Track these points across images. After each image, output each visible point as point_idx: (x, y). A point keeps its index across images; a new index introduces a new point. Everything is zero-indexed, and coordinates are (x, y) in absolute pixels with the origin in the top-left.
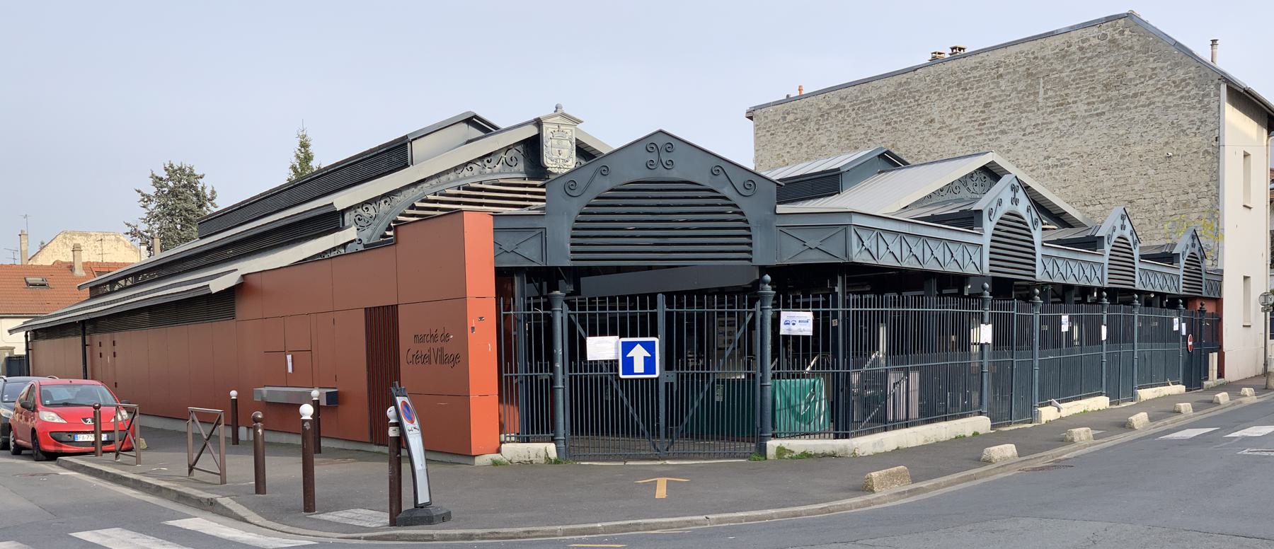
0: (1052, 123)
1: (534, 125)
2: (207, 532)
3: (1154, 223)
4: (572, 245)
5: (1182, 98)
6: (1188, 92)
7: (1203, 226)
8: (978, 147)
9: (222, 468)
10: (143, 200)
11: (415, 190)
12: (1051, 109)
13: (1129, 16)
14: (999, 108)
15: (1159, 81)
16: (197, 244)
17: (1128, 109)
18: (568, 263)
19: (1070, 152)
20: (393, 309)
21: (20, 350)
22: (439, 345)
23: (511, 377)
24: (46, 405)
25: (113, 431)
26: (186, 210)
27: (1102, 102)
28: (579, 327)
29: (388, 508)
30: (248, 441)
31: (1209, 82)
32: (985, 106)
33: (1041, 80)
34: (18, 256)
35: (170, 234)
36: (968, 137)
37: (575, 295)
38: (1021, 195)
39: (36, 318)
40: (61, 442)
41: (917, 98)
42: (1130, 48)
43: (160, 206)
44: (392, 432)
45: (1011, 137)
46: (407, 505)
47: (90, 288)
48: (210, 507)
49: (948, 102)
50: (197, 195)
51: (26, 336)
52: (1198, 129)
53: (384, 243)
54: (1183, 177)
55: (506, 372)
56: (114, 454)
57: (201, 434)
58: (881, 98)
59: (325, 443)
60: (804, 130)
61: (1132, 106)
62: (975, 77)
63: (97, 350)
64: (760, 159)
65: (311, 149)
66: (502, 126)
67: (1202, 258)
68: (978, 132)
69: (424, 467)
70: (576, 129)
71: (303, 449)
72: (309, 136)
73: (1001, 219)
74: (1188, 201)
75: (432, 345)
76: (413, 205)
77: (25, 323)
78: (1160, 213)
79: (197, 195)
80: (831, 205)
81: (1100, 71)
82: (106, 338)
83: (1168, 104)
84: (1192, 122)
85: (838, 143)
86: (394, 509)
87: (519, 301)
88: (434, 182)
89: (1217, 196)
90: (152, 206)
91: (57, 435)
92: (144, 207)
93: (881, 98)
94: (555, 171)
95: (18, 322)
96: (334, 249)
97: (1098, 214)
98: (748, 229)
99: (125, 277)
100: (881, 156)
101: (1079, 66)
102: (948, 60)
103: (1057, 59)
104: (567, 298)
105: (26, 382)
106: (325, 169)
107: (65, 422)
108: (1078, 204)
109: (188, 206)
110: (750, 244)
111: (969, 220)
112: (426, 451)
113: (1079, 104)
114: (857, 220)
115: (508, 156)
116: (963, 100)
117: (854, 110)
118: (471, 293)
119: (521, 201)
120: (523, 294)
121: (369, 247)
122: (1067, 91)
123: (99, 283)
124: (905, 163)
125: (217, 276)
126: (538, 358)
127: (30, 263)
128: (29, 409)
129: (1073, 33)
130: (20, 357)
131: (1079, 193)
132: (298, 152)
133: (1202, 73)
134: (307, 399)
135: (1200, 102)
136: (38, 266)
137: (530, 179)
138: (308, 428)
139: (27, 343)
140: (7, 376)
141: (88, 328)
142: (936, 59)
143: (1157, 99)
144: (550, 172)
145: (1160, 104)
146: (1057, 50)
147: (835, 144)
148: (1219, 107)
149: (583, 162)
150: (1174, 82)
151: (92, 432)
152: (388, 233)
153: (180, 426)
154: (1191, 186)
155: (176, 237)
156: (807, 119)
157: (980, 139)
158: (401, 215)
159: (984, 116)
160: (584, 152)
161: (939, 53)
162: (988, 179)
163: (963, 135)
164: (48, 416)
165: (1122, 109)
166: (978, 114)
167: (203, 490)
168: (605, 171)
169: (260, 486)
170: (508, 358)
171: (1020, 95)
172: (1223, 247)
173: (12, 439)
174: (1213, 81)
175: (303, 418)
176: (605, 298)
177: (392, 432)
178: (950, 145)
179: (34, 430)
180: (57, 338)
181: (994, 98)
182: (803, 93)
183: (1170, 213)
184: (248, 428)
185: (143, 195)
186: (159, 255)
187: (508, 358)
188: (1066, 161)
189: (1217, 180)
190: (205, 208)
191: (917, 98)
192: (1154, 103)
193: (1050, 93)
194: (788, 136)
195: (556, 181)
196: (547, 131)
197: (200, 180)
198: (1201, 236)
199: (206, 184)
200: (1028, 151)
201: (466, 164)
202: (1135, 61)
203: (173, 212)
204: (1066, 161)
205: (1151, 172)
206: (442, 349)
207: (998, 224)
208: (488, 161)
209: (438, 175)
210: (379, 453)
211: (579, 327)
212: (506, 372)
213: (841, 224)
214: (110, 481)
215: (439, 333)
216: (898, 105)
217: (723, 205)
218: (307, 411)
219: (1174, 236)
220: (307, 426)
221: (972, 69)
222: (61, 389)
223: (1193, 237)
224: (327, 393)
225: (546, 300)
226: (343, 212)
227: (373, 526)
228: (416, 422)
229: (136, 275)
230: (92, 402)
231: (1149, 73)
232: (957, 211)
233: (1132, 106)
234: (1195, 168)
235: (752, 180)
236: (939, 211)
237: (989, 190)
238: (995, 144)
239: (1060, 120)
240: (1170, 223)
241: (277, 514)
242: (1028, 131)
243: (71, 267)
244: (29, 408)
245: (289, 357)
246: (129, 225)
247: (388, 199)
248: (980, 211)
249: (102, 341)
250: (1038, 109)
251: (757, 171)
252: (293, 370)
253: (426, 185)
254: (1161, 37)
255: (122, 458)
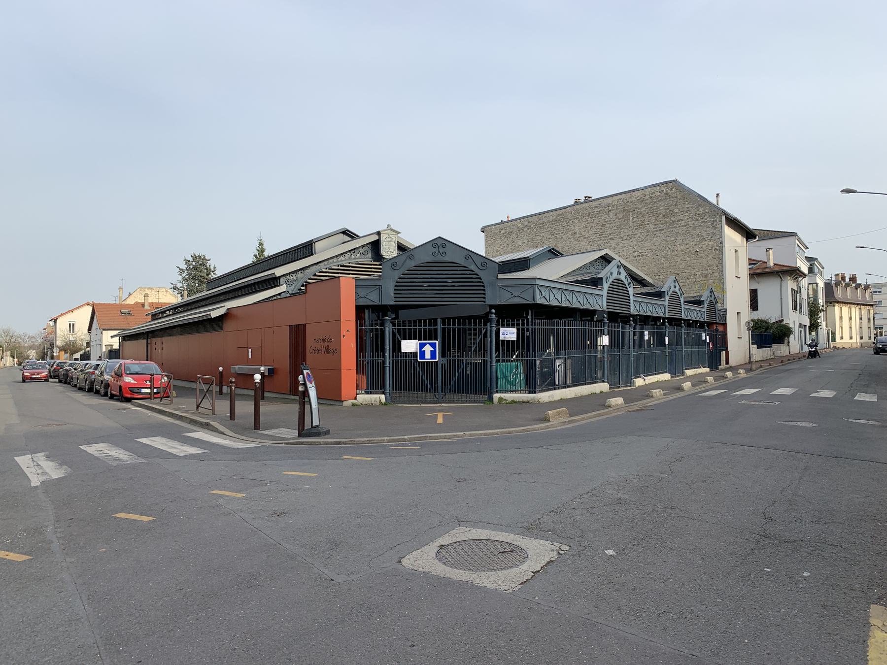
0: (636, 234)
1: (377, 234)
2: (204, 439)
3: (690, 285)
4: (394, 294)
5: (702, 222)
6: (706, 219)
7: (716, 286)
8: (599, 246)
9: (213, 407)
10: (180, 272)
11: (316, 267)
12: (636, 227)
13: (675, 181)
14: (609, 227)
15: (691, 214)
16: (205, 293)
17: (675, 227)
18: (392, 303)
19: (646, 249)
20: (304, 325)
21: (116, 346)
22: (326, 344)
23: (363, 360)
24: (127, 374)
25: (160, 388)
26: (201, 277)
27: (662, 224)
28: (397, 335)
29: (297, 428)
30: (227, 393)
31: (716, 215)
32: (602, 226)
33: (631, 213)
34: (117, 300)
35: (192, 288)
36: (593, 241)
37: (396, 319)
38: (622, 270)
39: (125, 330)
40: (134, 393)
41: (567, 222)
42: (676, 197)
43: (188, 275)
44: (301, 388)
45: (616, 241)
46: (307, 426)
47: (152, 315)
48: (206, 426)
49: (583, 224)
50: (207, 269)
51: (119, 339)
52: (711, 238)
53: (300, 293)
54: (705, 261)
55: (360, 358)
56: (160, 399)
57: (203, 390)
58: (549, 222)
59: (266, 395)
60: (510, 238)
61: (677, 226)
62: (597, 211)
63: (154, 346)
64: (488, 252)
65: (264, 246)
66: (361, 235)
67: (716, 303)
68: (599, 239)
69: (317, 406)
70: (398, 237)
71: (255, 397)
72: (263, 240)
73: (612, 282)
74: (708, 274)
75: (323, 344)
76: (315, 274)
77: (119, 332)
78: (694, 280)
79: (207, 269)
80: (525, 275)
81: (661, 208)
82: (158, 340)
83: (696, 225)
84: (708, 234)
85: (527, 244)
86: (300, 428)
87: (367, 322)
88: (326, 263)
89: (722, 271)
90: (184, 274)
91: (132, 389)
92: (180, 275)
93: (549, 222)
94: (387, 257)
95: (116, 332)
96: (274, 296)
97: (661, 280)
98: (484, 286)
99: (169, 310)
100: (550, 251)
101: (650, 206)
102: (583, 203)
103: (638, 202)
104: (392, 321)
105: (118, 362)
106: (271, 256)
107: (136, 382)
108: (651, 275)
109: (202, 274)
110: (484, 294)
111: (596, 282)
112: (318, 398)
113: (650, 225)
114: (539, 282)
115: (363, 250)
116: (591, 223)
117: (535, 228)
118: (343, 317)
119: (367, 272)
120: (369, 319)
121: (292, 295)
122: (644, 219)
123: (156, 313)
124: (562, 254)
125: (215, 309)
126: (377, 351)
127: (123, 303)
128: (118, 376)
129: (646, 190)
130: (116, 349)
131: (651, 270)
132: (258, 248)
133: (712, 210)
134: (258, 371)
135: (712, 224)
136: (127, 305)
137: (374, 261)
138: (258, 386)
139: (120, 342)
140: (109, 359)
141: (150, 335)
142: (577, 202)
143: (690, 223)
144: (384, 258)
145: (691, 225)
146: (639, 198)
147: (526, 245)
148: (721, 226)
149: (401, 253)
150: (698, 214)
151: (149, 388)
152: (302, 288)
153: (193, 385)
154: (708, 266)
155: (195, 290)
156: (511, 232)
157: (600, 242)
158: (309, 279)
159: (602, 231)
160: (401, 248)
161: (579, 200)
162: (604, 262)
163: (591, 240)
164: (128, 379)
165: (672, 228)
166: (598, 230)
167: (203, 418)
168: (411, 257)
169: (232, 416)
170: (361, 351)
171: (620, 220)
172: (726, 298)
173: (109, 391)
174: (718, 214)
175: (255, 381)
176: (411, 321)
177: (301, 388)
178: (584, 246)
179: (120, 387)
180: (135, 340)
181: (606, 222)
182: (510, 219)
183: (698, 280)
184: (228, 386)
185: (180, 269)
186: (186, 299)
187: (361, 351)
188: (644, 253)
189: (722, 263)
190: (210, 276)
191: (567, 222)
192: (688, 225)
193: (635, 219)
194: (502, 241)
195: (387, 263)
196: (383, 237)
197: (208, 262)
198: (715, 291)
199: (211, 264)
200: (625, 248)
201: (342, 254)
202: (678, 204)
203: (194, 278)
204: (644, 253)
205: (688, 259)
206: (328, 346)
207: (611, 284)
208: (353, 253)
209: (328, 259)
210: (294, 399)
211: (397, 335)
212: (360, 358)
213: (531, 284)
214: (157, 413)
215: (327, 338)
216: (558, 225)
217: (470, 274)
218: (258, 377)
219: (701, 292)
220: (257, 385)
221: (596, 207)
222: (134, 365)
223: (711, 292)
224: (269, 369)
225: (381, 322)
226: (280, 277)
227: (289, 437)
228: (313, 383)
229: (174, 309)
230: (150, 372)
231: (686, 209)
232: (590, 278)
233: (677, 226)
234: (711, 257)
235: (485, 262)
236: (580, 278)
237: (605, 268)
238: (607, 245)
239: (641, 233)
240: (699, 285)
241: (241, 431)
242: (624, 238)
243: (143, 305)
244: (119, 375)
245: (250, 350)
246: (172, 284)
247: (302, 271)
248: (602, 278)
249: (156, 341)
250: (629, 227)
251: (486, 257)
252: (252, 357)
253: (322, 264)
254: (691, 192)
255: (164, 401)
